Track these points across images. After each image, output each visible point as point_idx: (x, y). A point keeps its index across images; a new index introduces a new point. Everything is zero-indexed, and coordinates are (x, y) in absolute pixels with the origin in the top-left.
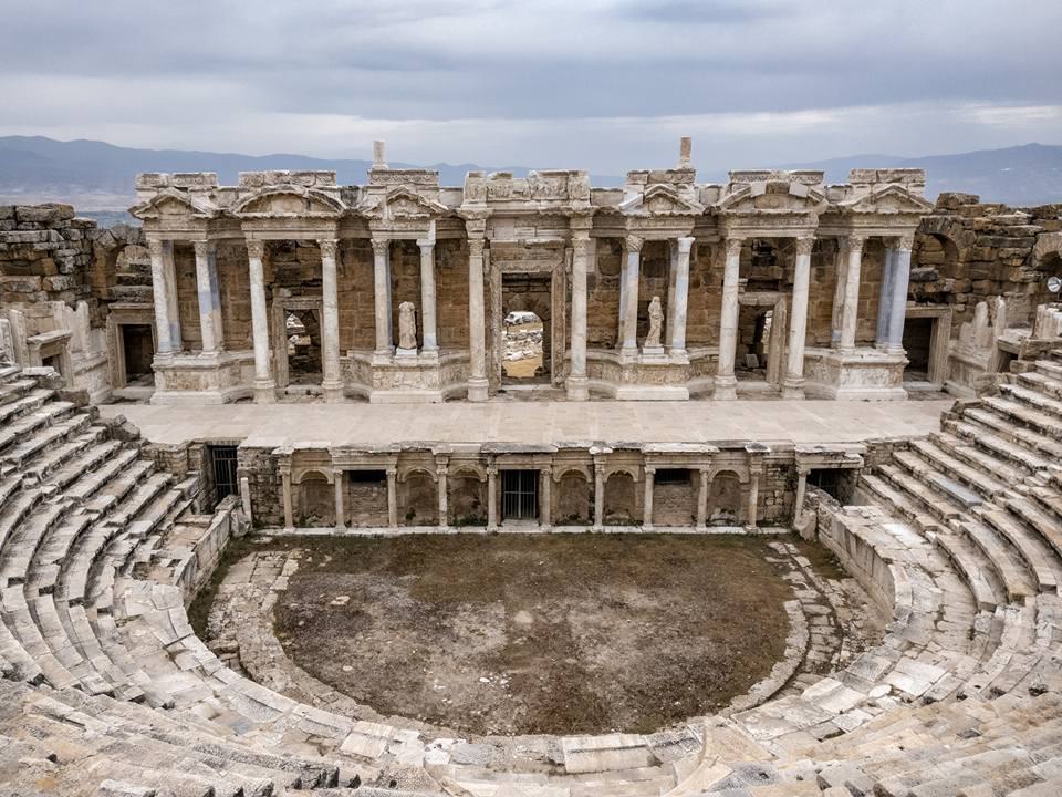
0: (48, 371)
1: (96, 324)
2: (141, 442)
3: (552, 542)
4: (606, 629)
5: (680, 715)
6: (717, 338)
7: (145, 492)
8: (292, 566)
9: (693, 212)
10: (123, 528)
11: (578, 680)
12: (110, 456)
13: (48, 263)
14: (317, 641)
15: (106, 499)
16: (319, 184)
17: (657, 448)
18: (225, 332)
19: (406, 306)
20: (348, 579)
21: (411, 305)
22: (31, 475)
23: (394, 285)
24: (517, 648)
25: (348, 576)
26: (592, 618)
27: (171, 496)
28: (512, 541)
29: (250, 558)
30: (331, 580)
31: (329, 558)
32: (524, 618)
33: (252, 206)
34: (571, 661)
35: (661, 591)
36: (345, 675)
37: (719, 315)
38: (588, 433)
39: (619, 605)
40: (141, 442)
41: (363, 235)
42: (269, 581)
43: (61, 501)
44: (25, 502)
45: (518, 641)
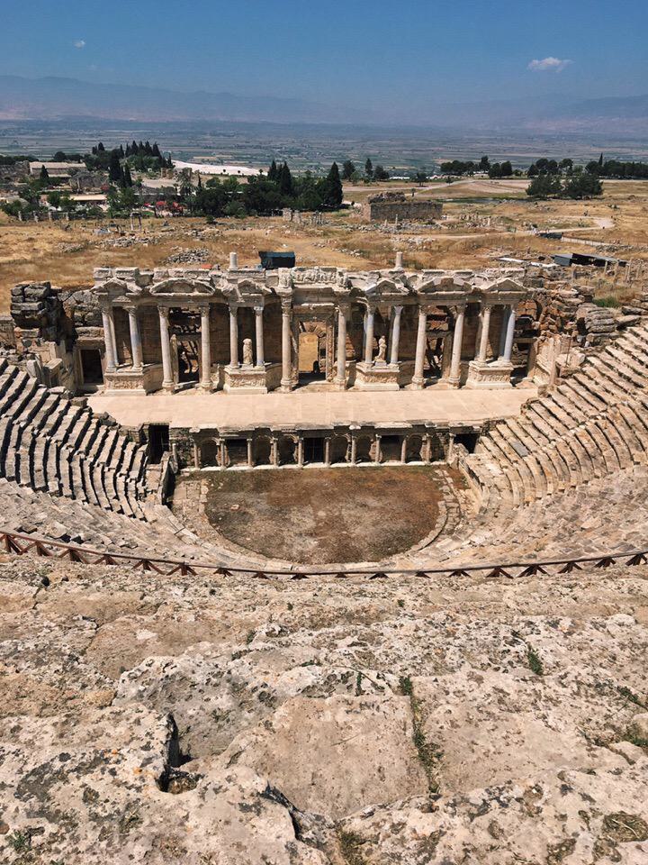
0: (60, 389)
1: (69, 350)
2: (117, 426)
3: (331, 473)
4: (359, 517)
5: (390, 554)
6: (415, 356)
7: (128, 452)
8: (205, 489)
9: (403, 294)
10: (128, 476)
11: (348, 541)
12: (106, 436)
13: (44, 319)
14: (230, 527)
15: (114, 463)
16: (200, 278)
17: (383, 425)
18: (143, 354)
19: (247, 341)
20: (234, 496)
21: (250, 340)
22: (80, 452)
23: (240, 328)
24: (321, 528)
25: (234, 494)
26: (352, 512)
27: (139, 456)
28: (312, 473)
29: (182, 485)
30: (227, 496)
31: (222, 484)
32: (322, 514)
33: (161, 289)
34: (345, 532)
35: (383, 498)
36: (248, 542)
37: (416, 343)
38: (347, 416)
39: (364, 505)
40: (117, 426)
41: (222, 301)
42: (198, 498)
43: (98, 466)
44: (87, 469)
45: (320, 524)
